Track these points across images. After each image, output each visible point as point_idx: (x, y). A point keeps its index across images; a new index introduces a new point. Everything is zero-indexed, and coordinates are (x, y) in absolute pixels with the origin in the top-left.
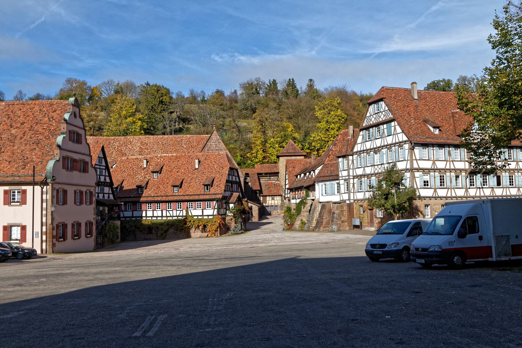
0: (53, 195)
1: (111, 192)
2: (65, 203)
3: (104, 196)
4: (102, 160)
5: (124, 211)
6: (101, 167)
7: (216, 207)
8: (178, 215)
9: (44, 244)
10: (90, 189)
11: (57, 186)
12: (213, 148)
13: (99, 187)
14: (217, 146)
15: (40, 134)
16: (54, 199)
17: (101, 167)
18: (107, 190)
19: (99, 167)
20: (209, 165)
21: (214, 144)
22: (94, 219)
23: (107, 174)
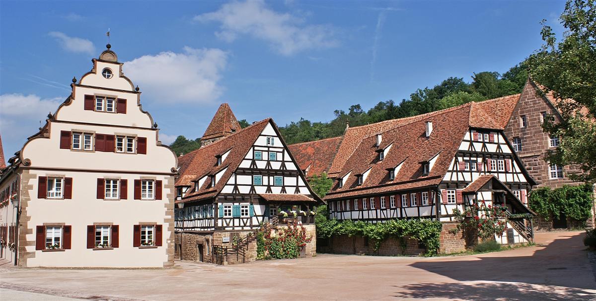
1: (301, 183)
2: (68, 195)
3: (284, 190)
4: (273, 140)
5: (345, 211)
6: (271, 149)
7: (434, 202)
8: (392, 217)
10: (155, 177)
11: (43, 174)
12: (531, 107)
13: (271, 178)
14: (537, 103)
16: (30, 191)
17: (271, 149)
18: (290, 181)
19: (267, 149)
20: (444, 129)
21: (531, 102)
23: (287, 157)
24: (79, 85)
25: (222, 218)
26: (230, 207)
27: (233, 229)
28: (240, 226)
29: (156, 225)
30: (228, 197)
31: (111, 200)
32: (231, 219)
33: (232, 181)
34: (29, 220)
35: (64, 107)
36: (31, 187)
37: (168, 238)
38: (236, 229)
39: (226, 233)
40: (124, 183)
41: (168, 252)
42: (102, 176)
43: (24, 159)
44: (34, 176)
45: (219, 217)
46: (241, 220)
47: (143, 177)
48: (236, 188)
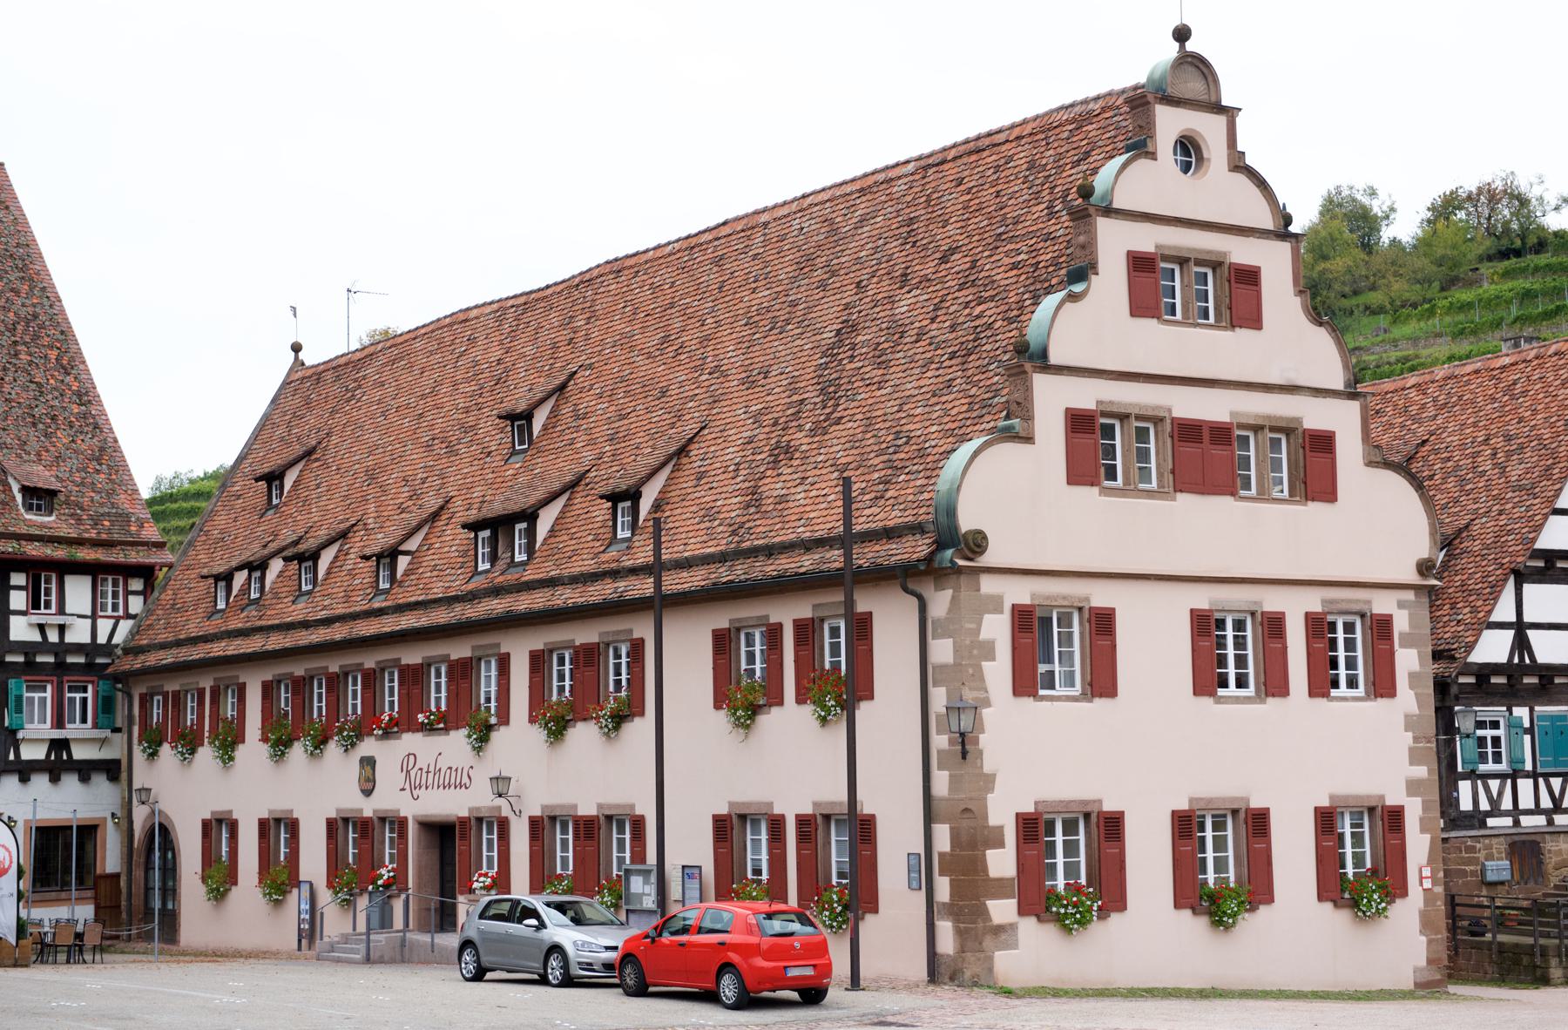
0: (985, 634)
2: (1102, 682)
9: (945, 928)
11: (1020, 592)
15: (992, 298)
16: (986, 665)
22: (1413, 787)
24: (1109, 211)
25: (1472, 775)
26: (1495, 725)
27: (1517, 823)
28: (1537, 810)
29: (1247, 810)
30: (1557, 681)
31: (1058, 699)
32: (1502, 776)
33: (1504, 610)
34: (992, 790)
35: (1068, 305)
36: (988, 651)
37: (1424, 862)
38: (1526, 821)
39: (1494, 841)
40: (1274, 626)
41: (1426, 924)
42: (1202, 598)
43: (963, 530)
44: (995, 604)
45: (1460, 769)
46: (1541, 780)
47: (1332, 602)
48: (1521, 644)
